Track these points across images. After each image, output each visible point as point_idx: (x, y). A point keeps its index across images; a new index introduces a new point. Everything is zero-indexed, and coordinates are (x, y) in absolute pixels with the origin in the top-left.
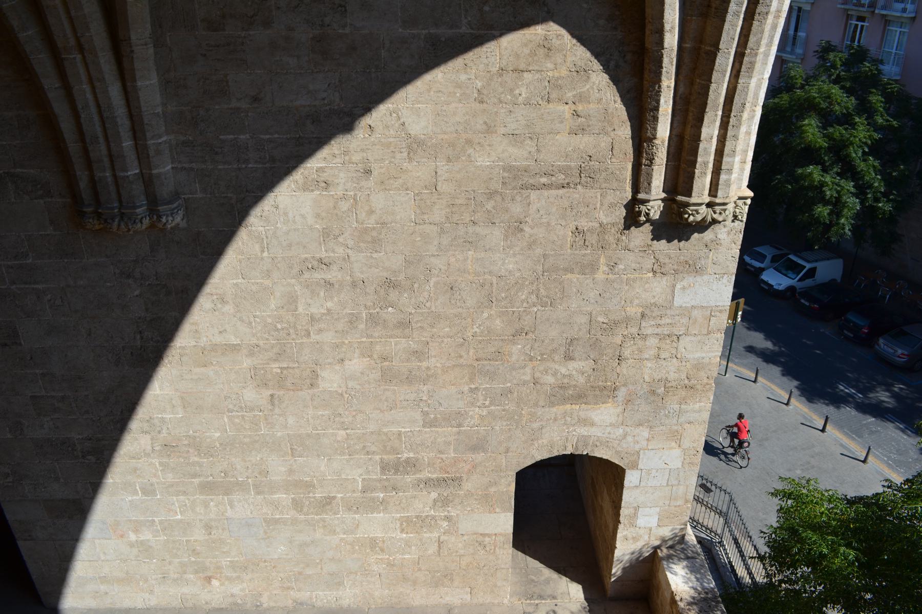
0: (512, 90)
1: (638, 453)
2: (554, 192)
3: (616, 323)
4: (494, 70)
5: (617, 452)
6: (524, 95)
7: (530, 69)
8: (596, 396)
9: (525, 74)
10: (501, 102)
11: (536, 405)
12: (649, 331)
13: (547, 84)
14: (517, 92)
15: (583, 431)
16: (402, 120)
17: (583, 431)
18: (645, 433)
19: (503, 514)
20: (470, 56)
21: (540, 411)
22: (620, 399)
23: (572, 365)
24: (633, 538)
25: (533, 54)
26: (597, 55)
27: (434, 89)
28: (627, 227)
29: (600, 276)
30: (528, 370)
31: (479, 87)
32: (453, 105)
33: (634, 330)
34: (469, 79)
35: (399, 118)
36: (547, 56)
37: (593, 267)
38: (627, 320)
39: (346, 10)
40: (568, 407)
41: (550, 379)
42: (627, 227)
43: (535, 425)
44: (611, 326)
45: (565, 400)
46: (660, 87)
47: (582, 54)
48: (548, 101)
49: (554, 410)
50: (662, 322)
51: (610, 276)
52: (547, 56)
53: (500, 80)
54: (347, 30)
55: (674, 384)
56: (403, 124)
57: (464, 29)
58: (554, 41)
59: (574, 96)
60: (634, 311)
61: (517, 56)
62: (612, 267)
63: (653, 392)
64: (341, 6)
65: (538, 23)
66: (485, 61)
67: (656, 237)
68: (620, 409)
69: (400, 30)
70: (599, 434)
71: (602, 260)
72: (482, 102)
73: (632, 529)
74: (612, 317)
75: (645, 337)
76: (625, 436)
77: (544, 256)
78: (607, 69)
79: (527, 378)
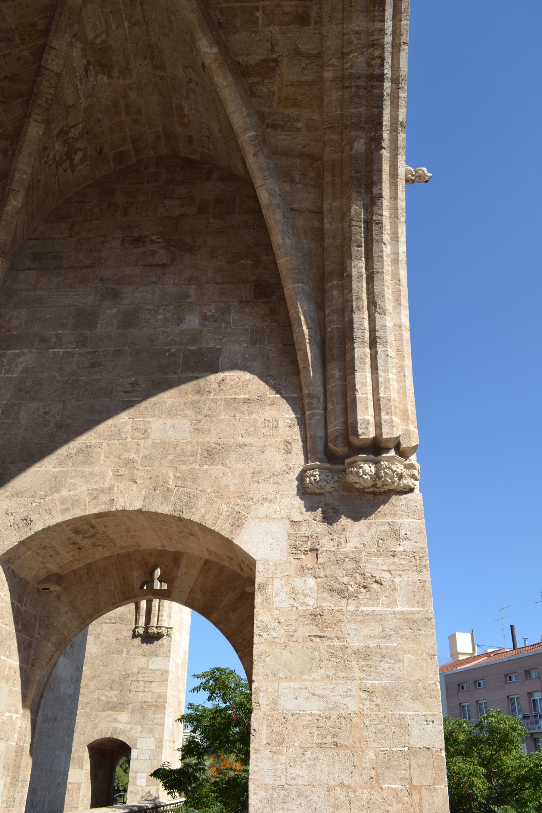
1: (137, 739)
2: (110, 625)
3: (129, 675)
5: (128, 738)
8: (120, 708)
11: (98, 711)
12: (140, 679)
15: (115, 725)
17: (115, 725)
18: (139, 728)
19: (79, 770)
21: (99, 713)
22: (129, 710)
23: (113, 693)
24: (135, 792)
28: (133, 638)
29: (124, 655)
30: (96, 693)
33: (135, 678)
37: (121, 652)
38: (133, 674)
40: (110, 712)
41: (103, 698)
42: (133, 638)
43: (97, 720)
44: (127, 676)
45: (109, 709)
49: (104, 713)
50: (145, 675)
51: (127, 656)
55: (150, 704)
60: (135, 670)
62: (128, 652)
63: (142, 708)
67: (143, 642)
68: (129, 715)
70: (121, 727)
71: (125, 650)
73: (134, 787)
74: (128, 672)
75: (138, 681)
76: (131, 728)
77: (106, 647)
79: (96, 697)
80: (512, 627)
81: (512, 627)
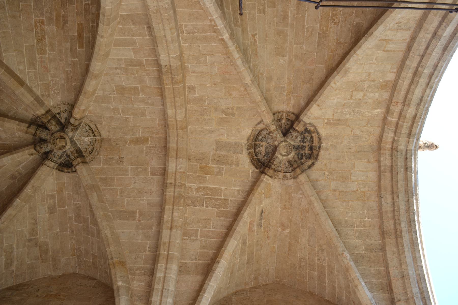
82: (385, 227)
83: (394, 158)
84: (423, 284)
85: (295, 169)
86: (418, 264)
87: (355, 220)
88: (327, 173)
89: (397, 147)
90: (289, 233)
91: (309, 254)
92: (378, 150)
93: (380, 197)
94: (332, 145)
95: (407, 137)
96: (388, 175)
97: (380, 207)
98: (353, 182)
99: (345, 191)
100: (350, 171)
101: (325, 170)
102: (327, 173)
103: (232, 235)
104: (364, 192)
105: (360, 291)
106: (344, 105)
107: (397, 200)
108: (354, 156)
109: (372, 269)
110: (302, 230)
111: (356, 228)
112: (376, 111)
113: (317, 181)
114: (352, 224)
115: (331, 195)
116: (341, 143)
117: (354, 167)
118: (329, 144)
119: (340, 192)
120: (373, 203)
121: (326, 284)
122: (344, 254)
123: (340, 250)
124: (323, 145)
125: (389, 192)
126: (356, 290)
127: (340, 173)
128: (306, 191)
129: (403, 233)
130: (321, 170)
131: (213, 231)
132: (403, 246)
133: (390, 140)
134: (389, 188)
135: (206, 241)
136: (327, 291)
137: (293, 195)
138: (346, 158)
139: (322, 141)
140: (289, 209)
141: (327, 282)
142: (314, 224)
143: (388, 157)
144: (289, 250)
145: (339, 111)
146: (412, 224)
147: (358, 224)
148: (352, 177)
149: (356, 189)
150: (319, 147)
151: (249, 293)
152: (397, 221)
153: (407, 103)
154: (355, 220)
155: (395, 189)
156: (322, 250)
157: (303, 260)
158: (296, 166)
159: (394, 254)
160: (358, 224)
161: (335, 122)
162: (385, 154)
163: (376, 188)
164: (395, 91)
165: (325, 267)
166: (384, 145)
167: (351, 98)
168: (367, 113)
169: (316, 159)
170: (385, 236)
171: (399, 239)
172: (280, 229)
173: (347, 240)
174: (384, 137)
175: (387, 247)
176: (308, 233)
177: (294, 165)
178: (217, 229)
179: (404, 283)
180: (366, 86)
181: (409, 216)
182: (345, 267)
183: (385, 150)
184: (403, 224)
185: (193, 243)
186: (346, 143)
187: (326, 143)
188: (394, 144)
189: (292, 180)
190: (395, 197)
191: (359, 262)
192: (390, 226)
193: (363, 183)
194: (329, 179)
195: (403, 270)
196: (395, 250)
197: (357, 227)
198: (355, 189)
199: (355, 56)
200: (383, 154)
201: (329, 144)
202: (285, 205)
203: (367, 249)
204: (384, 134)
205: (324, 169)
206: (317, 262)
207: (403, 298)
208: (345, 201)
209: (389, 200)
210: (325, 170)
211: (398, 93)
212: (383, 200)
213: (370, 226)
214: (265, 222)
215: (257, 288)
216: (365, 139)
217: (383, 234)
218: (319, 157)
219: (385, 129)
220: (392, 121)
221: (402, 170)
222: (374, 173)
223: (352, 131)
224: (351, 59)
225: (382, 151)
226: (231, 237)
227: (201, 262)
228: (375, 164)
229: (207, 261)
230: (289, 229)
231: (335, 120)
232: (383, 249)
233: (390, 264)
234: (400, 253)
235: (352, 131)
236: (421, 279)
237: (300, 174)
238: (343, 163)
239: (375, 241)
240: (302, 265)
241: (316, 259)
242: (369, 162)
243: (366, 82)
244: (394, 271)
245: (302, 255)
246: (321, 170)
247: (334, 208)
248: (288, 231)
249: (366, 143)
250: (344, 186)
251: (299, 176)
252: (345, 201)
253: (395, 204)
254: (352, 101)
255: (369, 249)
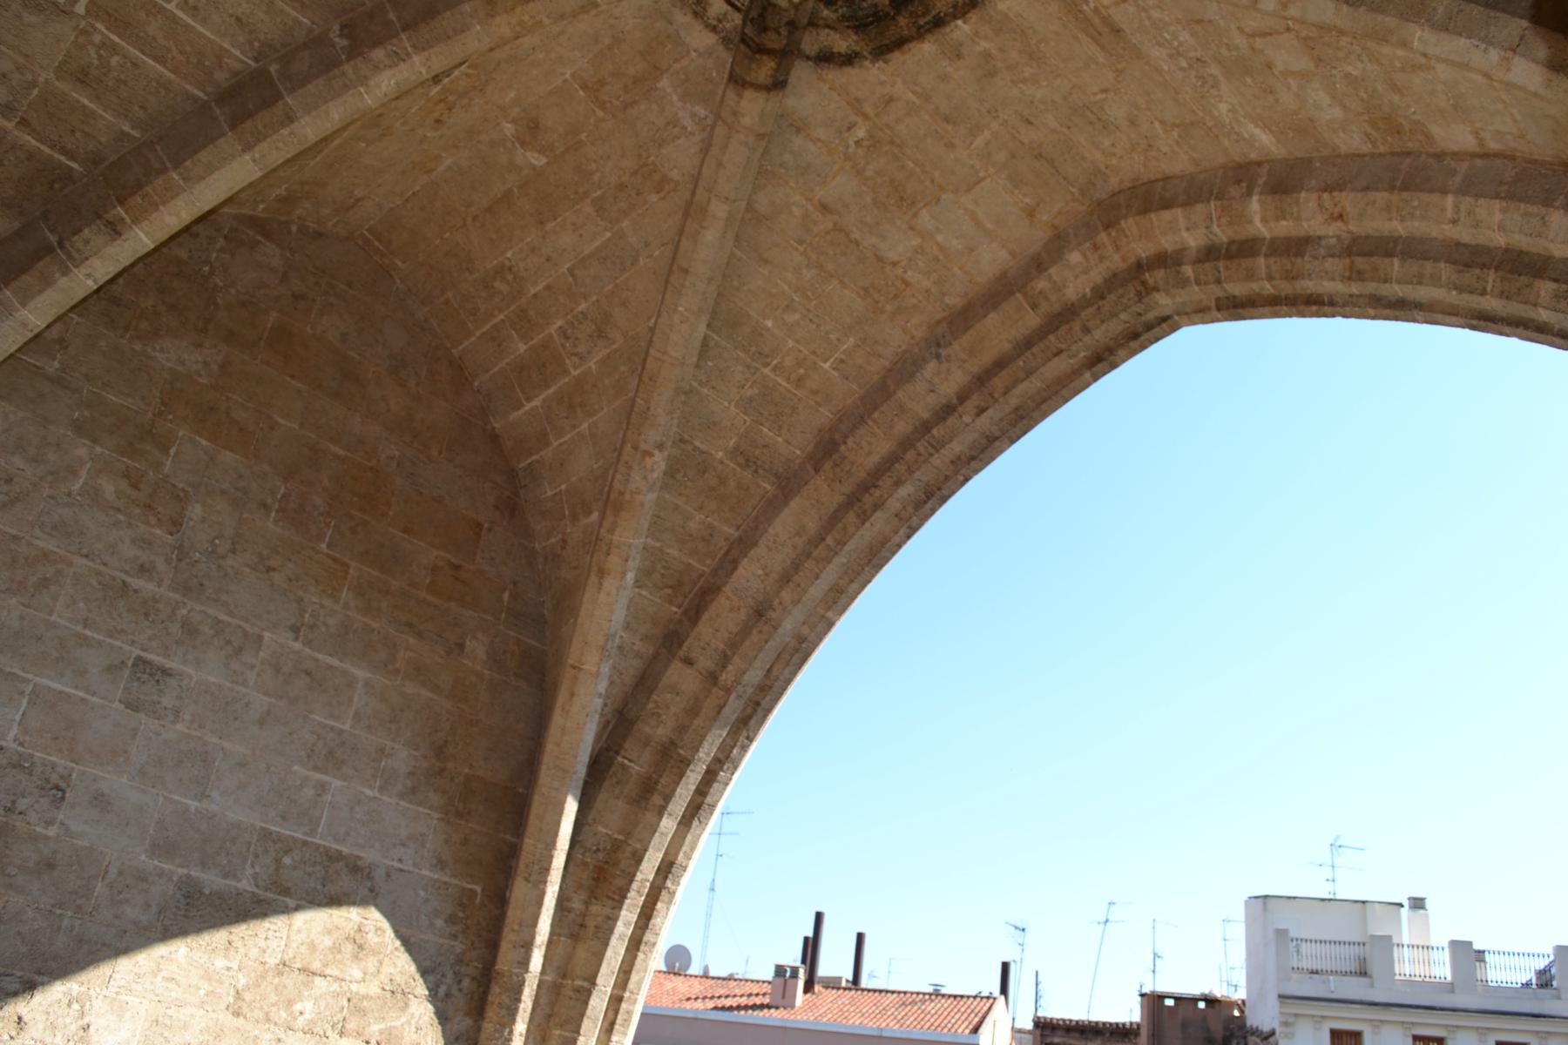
0: (290, 1003)
4: (272, 961)
6: (307, 1016)
7: (328, 972)
9: (318, 980)
10: (268, 1020)
13: (345, 1003)
14: (298, 1007)
16: (86, 1020)
20: (241, 931)
25: (336, 949)
26: (424, 972)
27: (164, 973)
31: (240, 987)
32: (189, 1010)
34: (229, 969)
35: (83, 1015)
36: (356, 957)
39: (63, 798)
46: (511, 1032)
47: (402, 966)
48: (341, 1034)
52: (356, 957)
53: (276, 980)
54: (52, 832)
56: (86, 1028)
57: (245, 885)
58: (370, 936)
59: (381, 1032)
61: (312, 946)
64: (57, 788)
65: (354, 903)
66: (263, 944)
69: (143, 857)
72: (237, 1014)
78: (433, 996)
80: (1005, 967)
81: (1005, 967)
82: (850, 441)
83: (1106, 305)
84: (786, 671)
85: (763, 50)
86: (830, 614)
87: (791, 343)
88: (861, 133)
89: (1156, 289)
90: (534, 168)
91: (548, 287)
92: (1100, 203)
93: (935, 345)
94: (987, 55)
95: (1218, 299)
96: (1032, 320)
97: (904, 369)
98: (912, 228)
99: (856, 235)
100: (941, 188)
101: (866, 116)
102: (861, 133)
103: (259, 138)
104: (907, 284)
105: (602, 597)
106: (1199, 22)
107: (967, 419)
108: (1013, 156)
109: (699, 517)
110: (589, 210)
111: (767, 371)
112: (1257, 131)
113: (798, 130)
114: (766, 350)
115: (797, 211)
116: (1024, 81)
117: (968, 190)
118: (984, 44)
119: (837, 228)
120: (896, 338)
121: (529, 399)
122: (651, 455)
123: (652, 436)
124: (961, 29)
125: (975, 366)
126: (594, 579)
127: (903, 167)
128: (720, 164)
129: (878, 514)
130: (856, 104)
131: (174, 19)
132: (842, 543)
133: (1168, 243)
134: (987, 358)
135: (114, 49)
136: (514, 416)
137: (664, 83)
138: (979, 141)
139: (973, 16)
140: (602, 106)
141: (536, 402)
142: (647, 245)
143: (1097, 275)
144: (489, 209)
145: (1155, 14)
146: (929, 505)
147: (788, 362)
148: (924, 213)
149: (896, 258)
150: (938, 23)
151: (221, 243)
152: (900, 467)
153: (1360, 262)
154: (791, 343)
155: (999, 382)
156: (601, 334)
157: (510, 277)
158: (776, 46)
159: (798, 534)
160: (788, 362)
161: (1097, 21)
162: (1102, 259)
163: (955, 300)
164: (1392, 188)
165: (566, 372)
166: (1135, 230)
167: (1253, 35)
168: (1223, 107)
169: (881, 52)
170: (828, 465)
171: (851, 517)
172: (508, 128)
173: (705, 391)
174: (1167, 215)
175: (797, 499)
176: (597, 243)
177: (772, 35)
178: (204, 21)
179: (745, 631)
180: (1350, 69)
181: (947, 478)
182: (621, 494)
183: (1118, 248)
184: (905, 491)
185: (33, 19)
186: (1038, 96)
187: (976, 34)
188: (1160, 274)
189: (710, 39)
190: (970, 405)
191: (679, 476)
192: (870, 453)
193: (938, 260)
194: (847, 157)
195: (776, 602)
196: (812, 525)
197: (774, 370)
198: (892, 255)
199: (1494, 55)
200: (1095, 247)
201: (984, 44)
202: (602, 83)
203: (737, 451)
204: (1178, 212)
205: (868, 109)
206: (553, 329)
207: (705, 663)
208: (820, 267)
209: (949, 387)
210: (866, 116)
211: (1388, 208)
212: (932, 366)
213: (815, 392)
214: (468, 75)
215: (268, 236)
216: (1107, 143)
217: (827, 448)
218: (896, 56)
219: (1199, 207)
220: (1251, 222)
221: (1082, 354)
222: (1003, 254)
223: (1105, 91)
224: (1463, 42)
225: (1103, 237)
226: (248, 148)
227: (29, 140)
228: (1034, 237)
229: (64, 151)
230: (545, 160)
231: (1106, 20)
232: (788, 484)
233: (760, 551)
234: (816, 547)
235: (1105, 91)
236: (799, 652)
237: (758, 87)
238: (950, 146)
239: (790, 445)
240: (497, 284)
241: (560, 323)
242: (1031, 213)
243: (1370, 67)
244: (750, 576)
245: (522, 265)
246: (856, 104)
247: (766, 262)
248: (539, 161)
249: (1097, 155)
250: (868, 219)
251: (749, 94)
252: (820, 267)
253: (951, 421)
254: (1240, 40)
255: (745, 456)
